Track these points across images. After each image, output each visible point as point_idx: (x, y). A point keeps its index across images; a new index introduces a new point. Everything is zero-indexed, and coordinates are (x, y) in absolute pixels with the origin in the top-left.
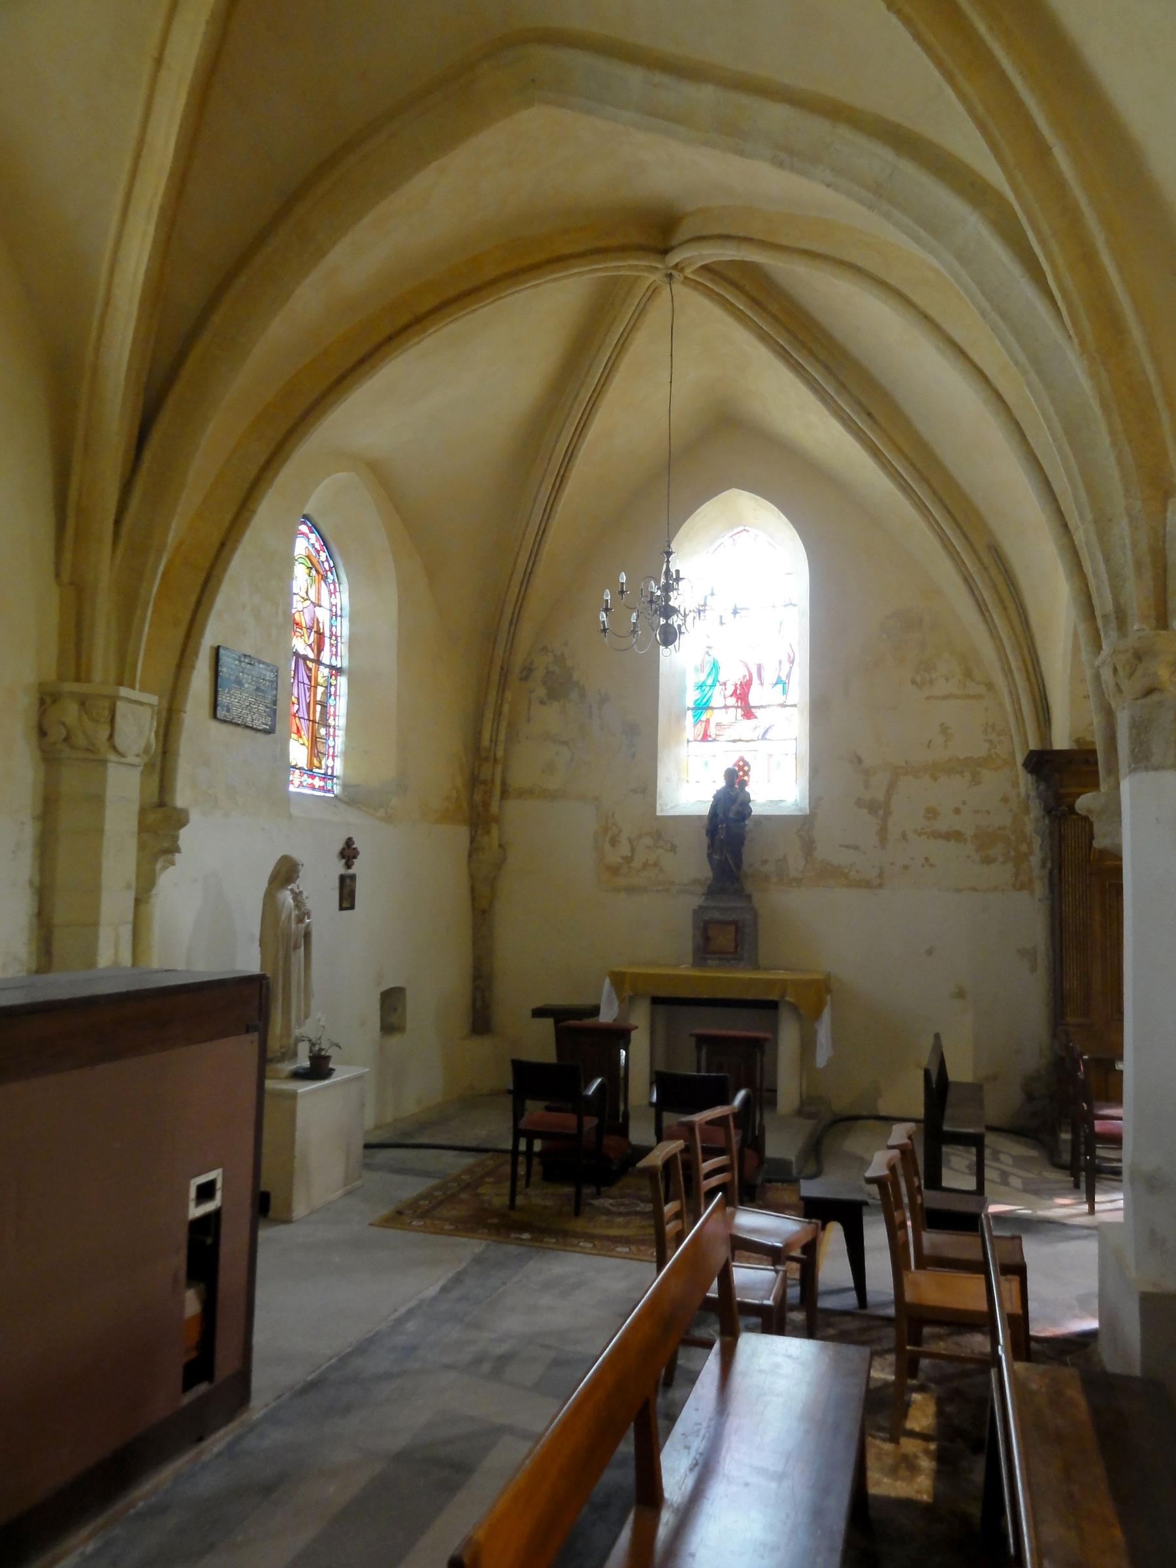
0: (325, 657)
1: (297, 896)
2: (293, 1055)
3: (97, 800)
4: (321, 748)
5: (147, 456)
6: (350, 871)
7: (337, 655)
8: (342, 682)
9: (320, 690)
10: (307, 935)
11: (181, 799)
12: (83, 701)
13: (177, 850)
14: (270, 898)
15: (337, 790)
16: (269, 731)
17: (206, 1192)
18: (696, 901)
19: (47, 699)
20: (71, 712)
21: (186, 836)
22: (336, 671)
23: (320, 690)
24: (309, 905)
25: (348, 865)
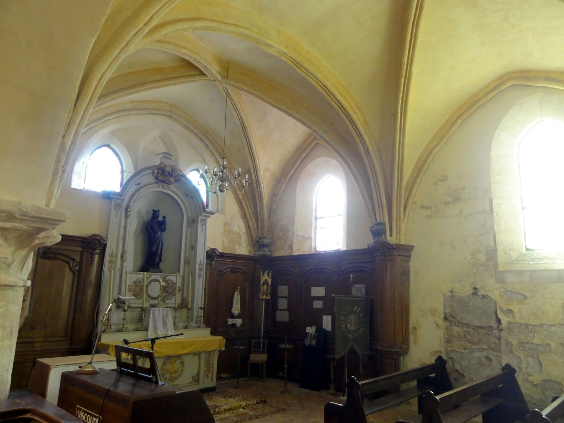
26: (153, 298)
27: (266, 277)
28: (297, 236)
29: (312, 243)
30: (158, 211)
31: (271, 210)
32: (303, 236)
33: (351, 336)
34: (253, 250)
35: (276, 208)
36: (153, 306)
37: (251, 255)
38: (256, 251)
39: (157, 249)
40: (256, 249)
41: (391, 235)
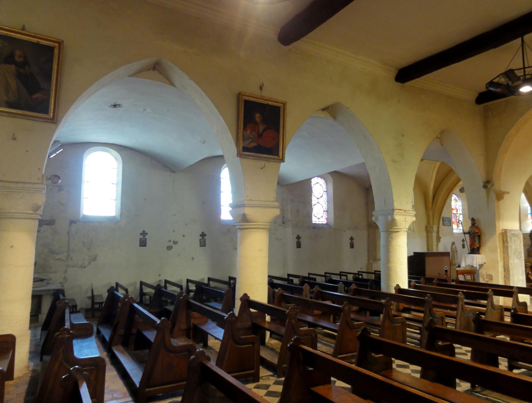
0: (458, 212)
1: (455, 247)
2: (456, 265)
3: (432, 236)
6: (463, 243)
7: (460, 212)
8: (461, 216)
9: (458, 218)
10: (457, 251)
11: (440, 235)
12: (430, 227)
14: (452, 247)
16: (450, 226)
17: (446, 268)
19: (426, 227)
21: (441, 240)
22: (460, 214)
24: (457, 247)
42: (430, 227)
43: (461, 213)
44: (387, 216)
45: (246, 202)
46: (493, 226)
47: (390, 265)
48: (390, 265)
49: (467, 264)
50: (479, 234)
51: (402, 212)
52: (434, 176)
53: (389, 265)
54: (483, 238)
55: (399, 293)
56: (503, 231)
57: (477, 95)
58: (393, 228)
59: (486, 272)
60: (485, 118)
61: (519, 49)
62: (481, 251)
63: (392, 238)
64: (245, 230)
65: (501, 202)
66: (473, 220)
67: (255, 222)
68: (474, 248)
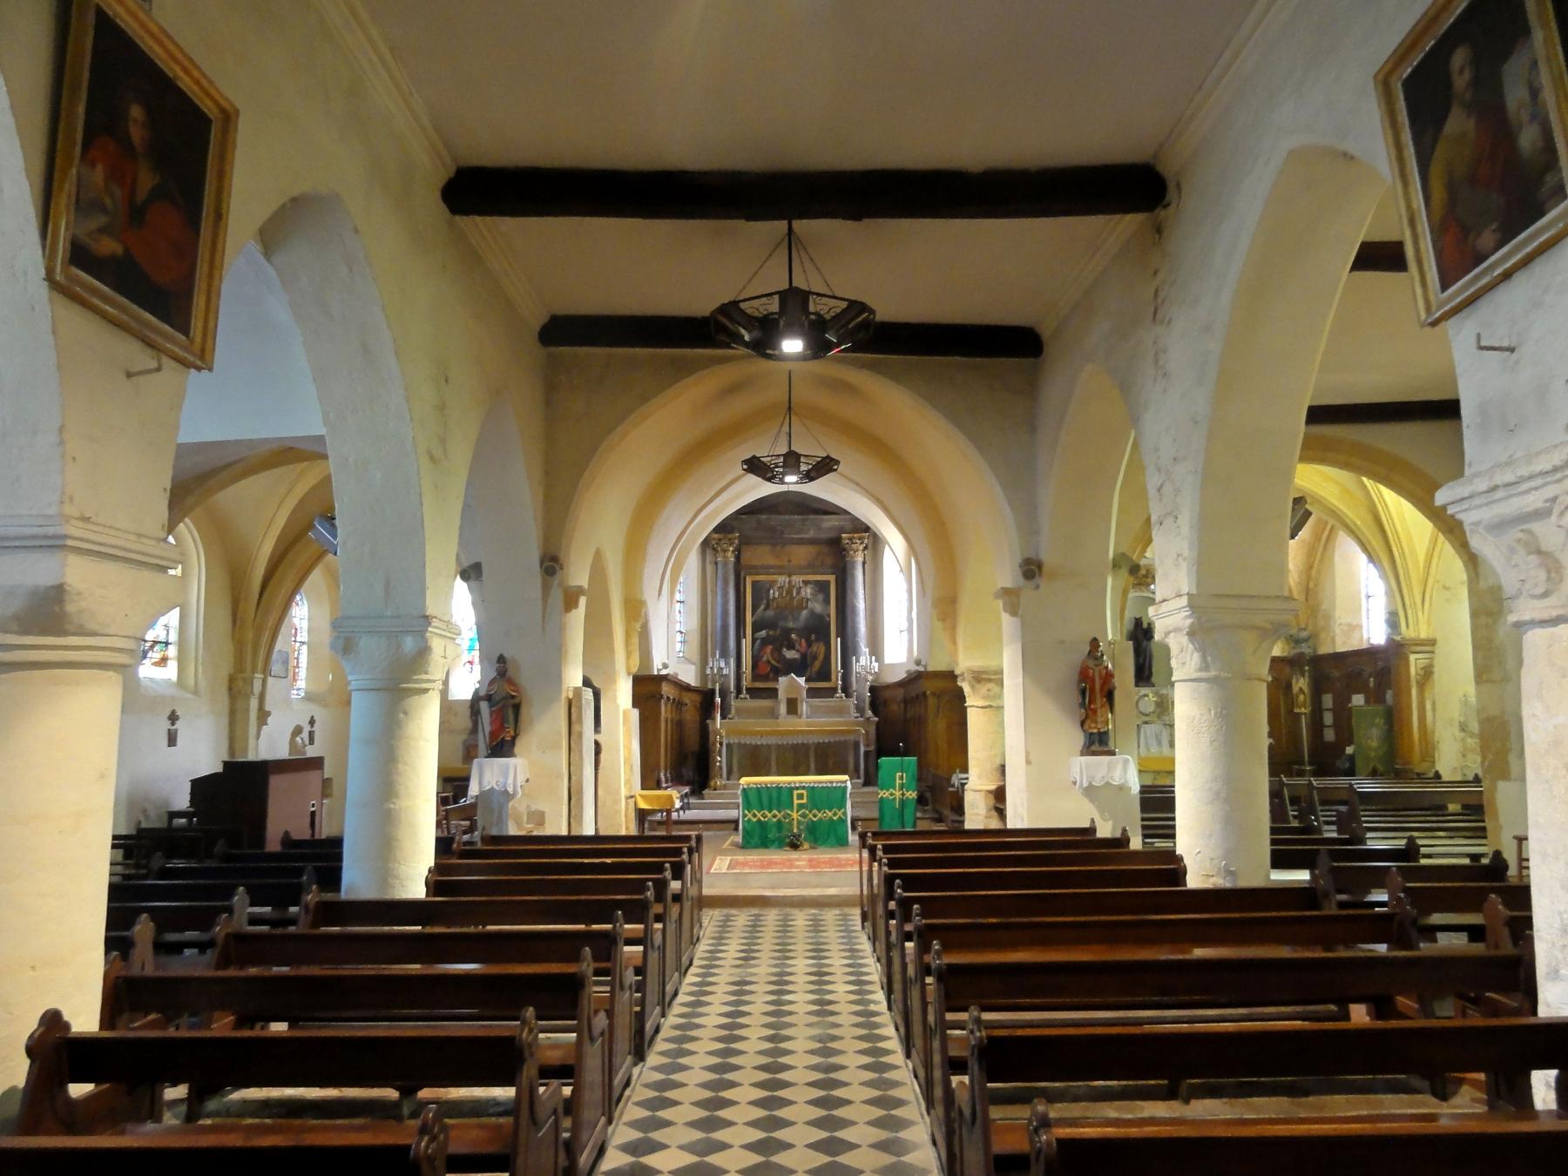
0: (298, 639)
3: (247, 710)
4: (296, 678)
5: (264, 598)
8: (304, 649)
9: (296, 653)
11: (267, 708)
12: (244, 680)
13: (266, 724)
15: (303, 694)
17: (313, 805)
18: (465, 736)
19: (232, 680)
20: (240, 684)
21: (270, 720)
22: (303, 643)
23: (296, 653)
25: (312, 726)
26: (1147, 715)
27: (1301, 684)
28: (1341, 624)
29: (1362, 634)
30: (1141, 618)
31: (1308, 592)
32: (1350, 625)
33: (1373, 754)
34: (1287, 648)
35: (1316, 585)
36: (1146, 723)
37: (1285, 654)
38: (1294, 648)
39: (1145, 660)
40: (1292, 645)
41: (1408, 626)
42: (244, 680)
43: (305, 639)
44: (397, 637)
45: (74, 529)
46: (555, 676)
47: (394, 803)
48: (394, 803)
49: (488, 788)
50: (516, 701)
51: (441, 626)
52: (281, 521)
53: (392, 806)
54: (524, 711)
55: (435, 896)
56: (571, 696)
57: (545, 319)
58: (415, 677)
59: (528, 806)
60: (551, 387)
61: (782, 240)
62: (517, 749)
63: (406, 713)
64: (20, 674)
65: (568, 614)
66: (501, 659)
67: (94, 634)
68: (503, 738)
